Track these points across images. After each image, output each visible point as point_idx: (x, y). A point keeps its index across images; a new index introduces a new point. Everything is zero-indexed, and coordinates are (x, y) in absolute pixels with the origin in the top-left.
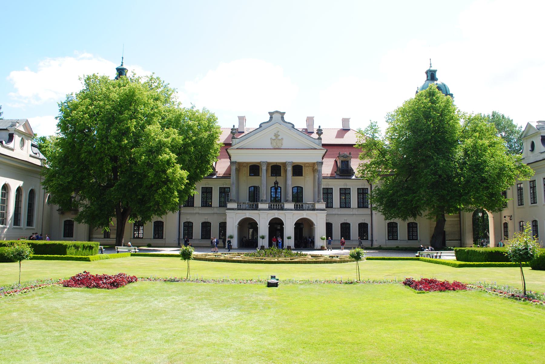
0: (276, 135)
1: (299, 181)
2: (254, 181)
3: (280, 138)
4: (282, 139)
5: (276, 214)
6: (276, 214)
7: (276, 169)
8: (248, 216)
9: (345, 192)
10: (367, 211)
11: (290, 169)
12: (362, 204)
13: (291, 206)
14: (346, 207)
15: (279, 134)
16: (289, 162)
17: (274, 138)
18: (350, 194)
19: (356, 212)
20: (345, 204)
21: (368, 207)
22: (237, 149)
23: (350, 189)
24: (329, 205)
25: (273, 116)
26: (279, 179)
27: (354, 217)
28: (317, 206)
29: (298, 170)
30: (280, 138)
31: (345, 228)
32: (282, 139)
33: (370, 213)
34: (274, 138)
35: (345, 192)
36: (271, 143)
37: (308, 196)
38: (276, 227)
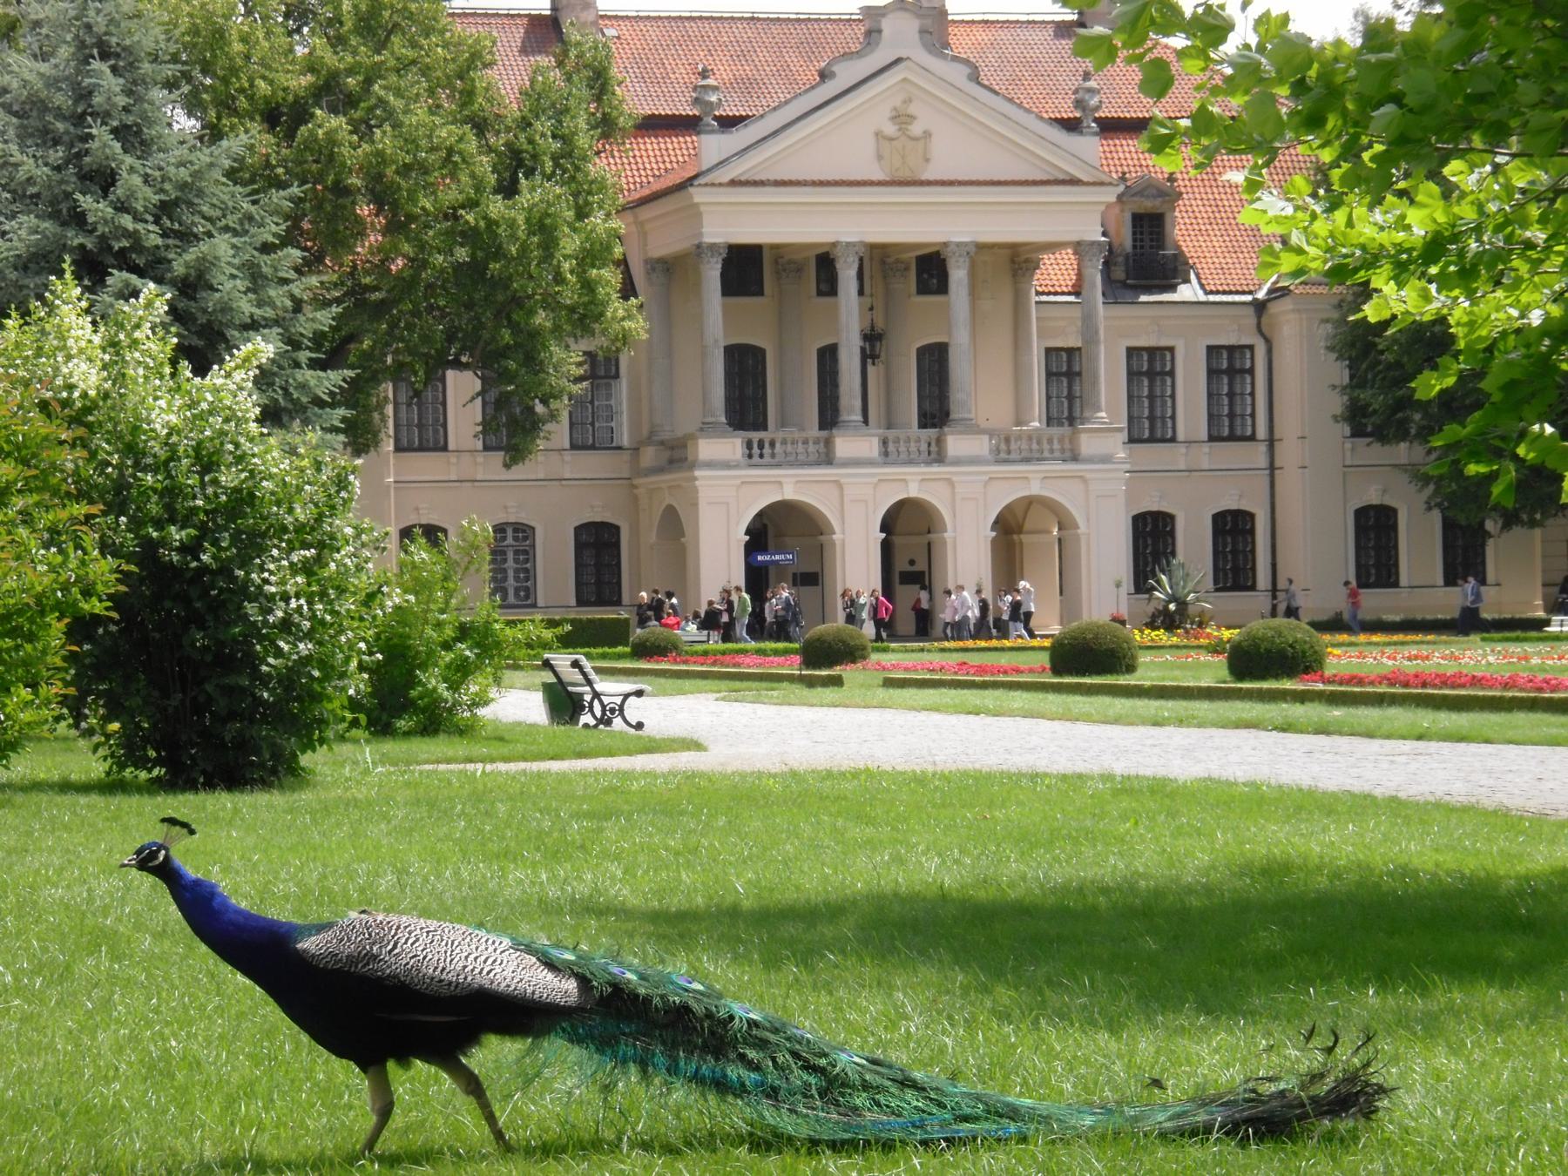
0: (901, 118)
2: (754, 323)
3: (916, 129)
4: (927, 135)
5: (914, 482)
6: (914, 482)
8: (789, 493)
9: (1150, 368)
10: (1256, 455)
14: (1152, 439)
15: (913, 109)
16: (958, 244)
17: (890, 129)
18: (1172, 373)
19: (1207, 456)
21: (1252, 438)
22: (733, 183)
23: (1171, 349)
25: (887, 25)
30: (916, 129)
32: (927, 135)
33: (1263, 462)
34: (890, 129)
36: (880, 157)
38: (908, 536)
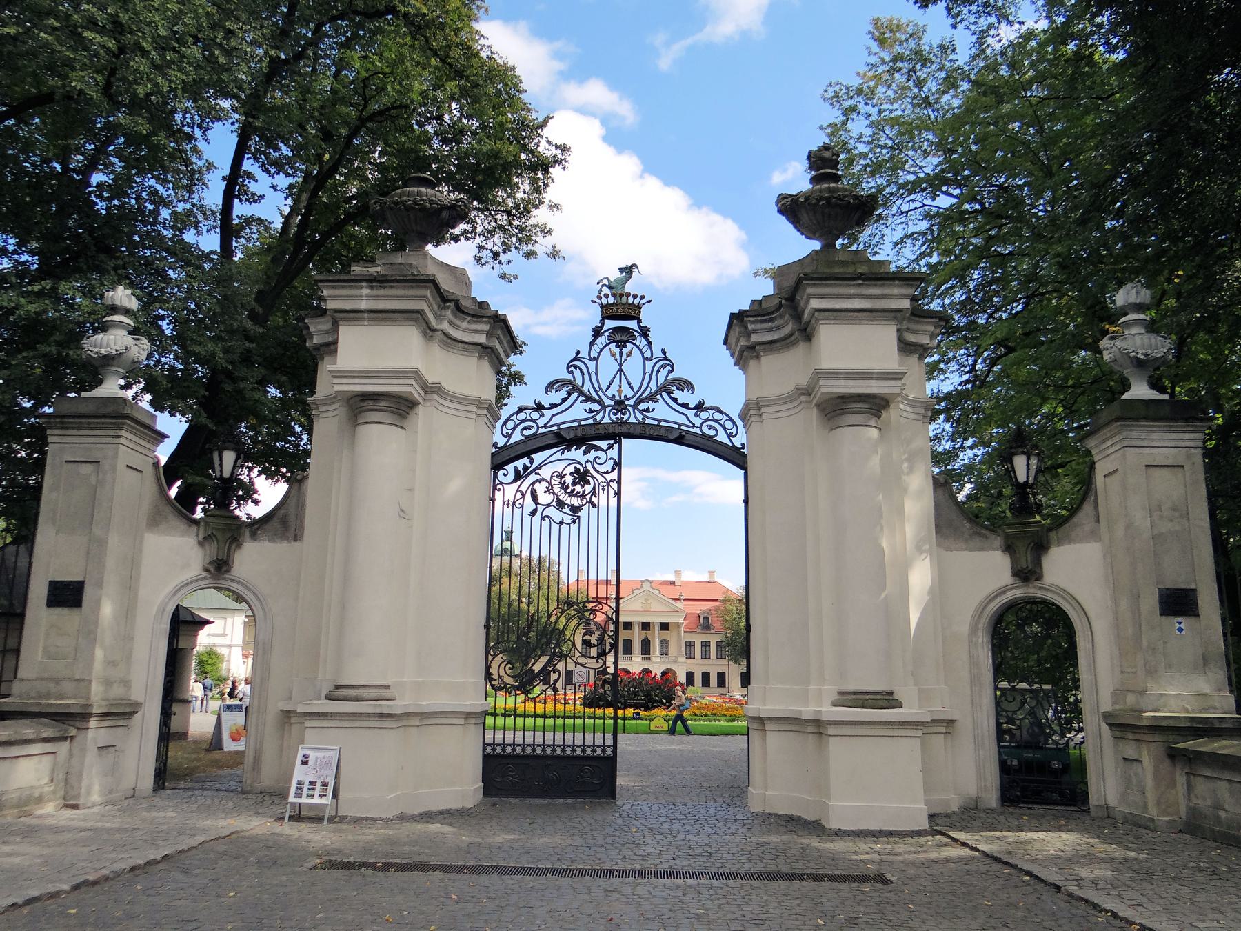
1: (666, 635)
7: (646, 626)
9: (706, 645)
10: (725, 662)
11: (657, 628)
12: (720, 657)
13: (659, 660)
20: (706, 655)
24: (690, 655)
26: (648, 634)
27: (715, 666)
28: (680, 659)
29: (664, 626)
31: (706, 677)
35: (706, 645)
37: (672, 649)
